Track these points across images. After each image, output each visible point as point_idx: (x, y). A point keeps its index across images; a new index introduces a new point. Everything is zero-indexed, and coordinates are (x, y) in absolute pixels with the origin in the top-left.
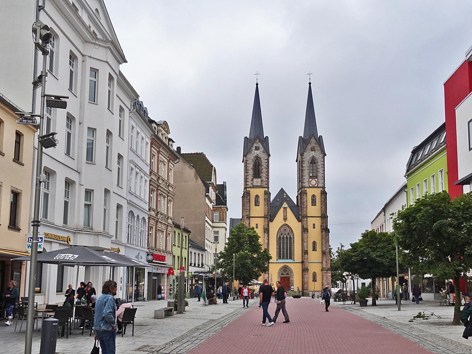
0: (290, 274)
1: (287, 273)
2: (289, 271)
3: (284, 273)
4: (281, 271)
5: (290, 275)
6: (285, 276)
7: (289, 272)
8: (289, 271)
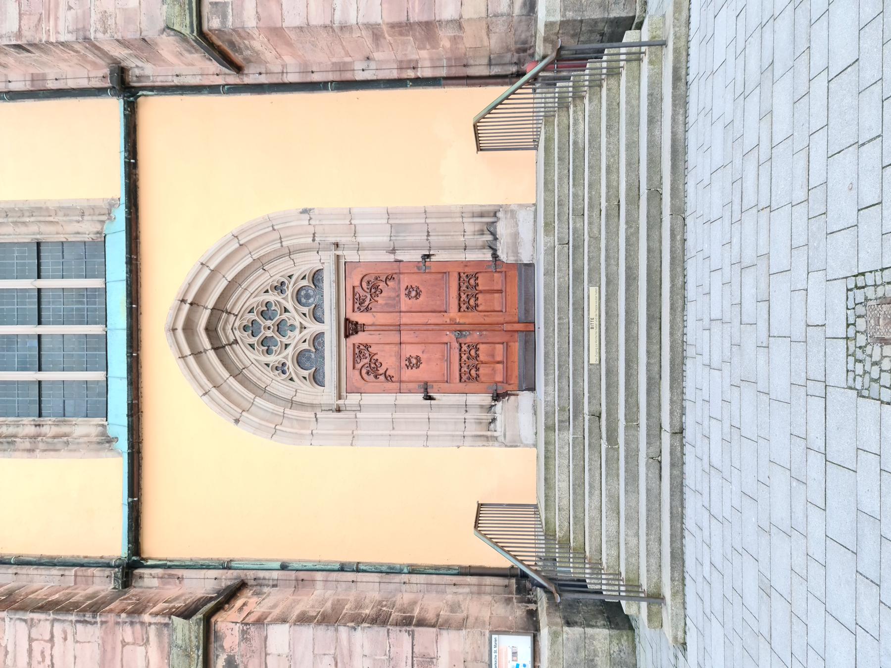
0: (307, 263)
1: (299, 297)
2: (263, 280)
3: (296, 340)
4: (274, 377)
5: (326, 261)
6: (329, 328)
7: (277, 271)
8: (263, 280)
